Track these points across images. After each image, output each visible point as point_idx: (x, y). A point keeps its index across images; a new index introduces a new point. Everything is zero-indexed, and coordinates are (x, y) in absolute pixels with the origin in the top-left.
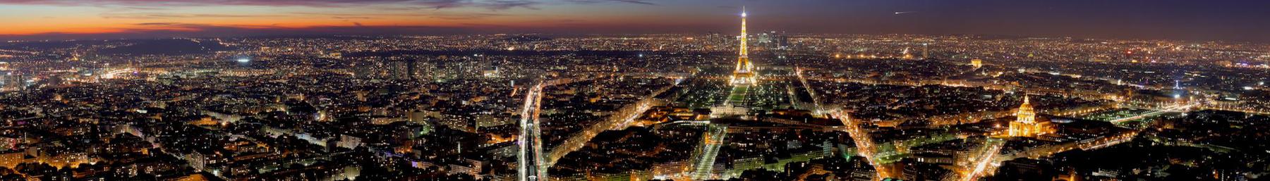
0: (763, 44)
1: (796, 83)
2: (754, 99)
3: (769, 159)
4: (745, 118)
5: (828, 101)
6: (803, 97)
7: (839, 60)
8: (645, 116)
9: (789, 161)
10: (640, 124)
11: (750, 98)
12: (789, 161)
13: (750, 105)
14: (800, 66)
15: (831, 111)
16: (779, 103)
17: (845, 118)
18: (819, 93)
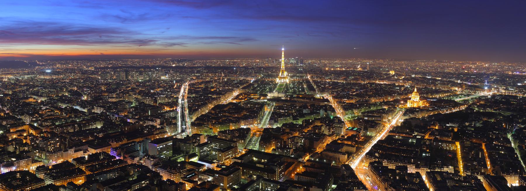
0: (292, 63)
1: (308, 82)
2: (288, 90)
3: (295, 118)
4: (283, 98)
5: (322, 91)
6: (311, 88)
7: (328, 71)
8: (237, 97)
9: (305, 119)
10: (234, 101)
11: (285, 88)
12: (305, 119)
13: (286, 92)
14: (309, 74)
15: (324, 95)
16: (299, 91)
17: (330, 98)
18: (318, 86)
